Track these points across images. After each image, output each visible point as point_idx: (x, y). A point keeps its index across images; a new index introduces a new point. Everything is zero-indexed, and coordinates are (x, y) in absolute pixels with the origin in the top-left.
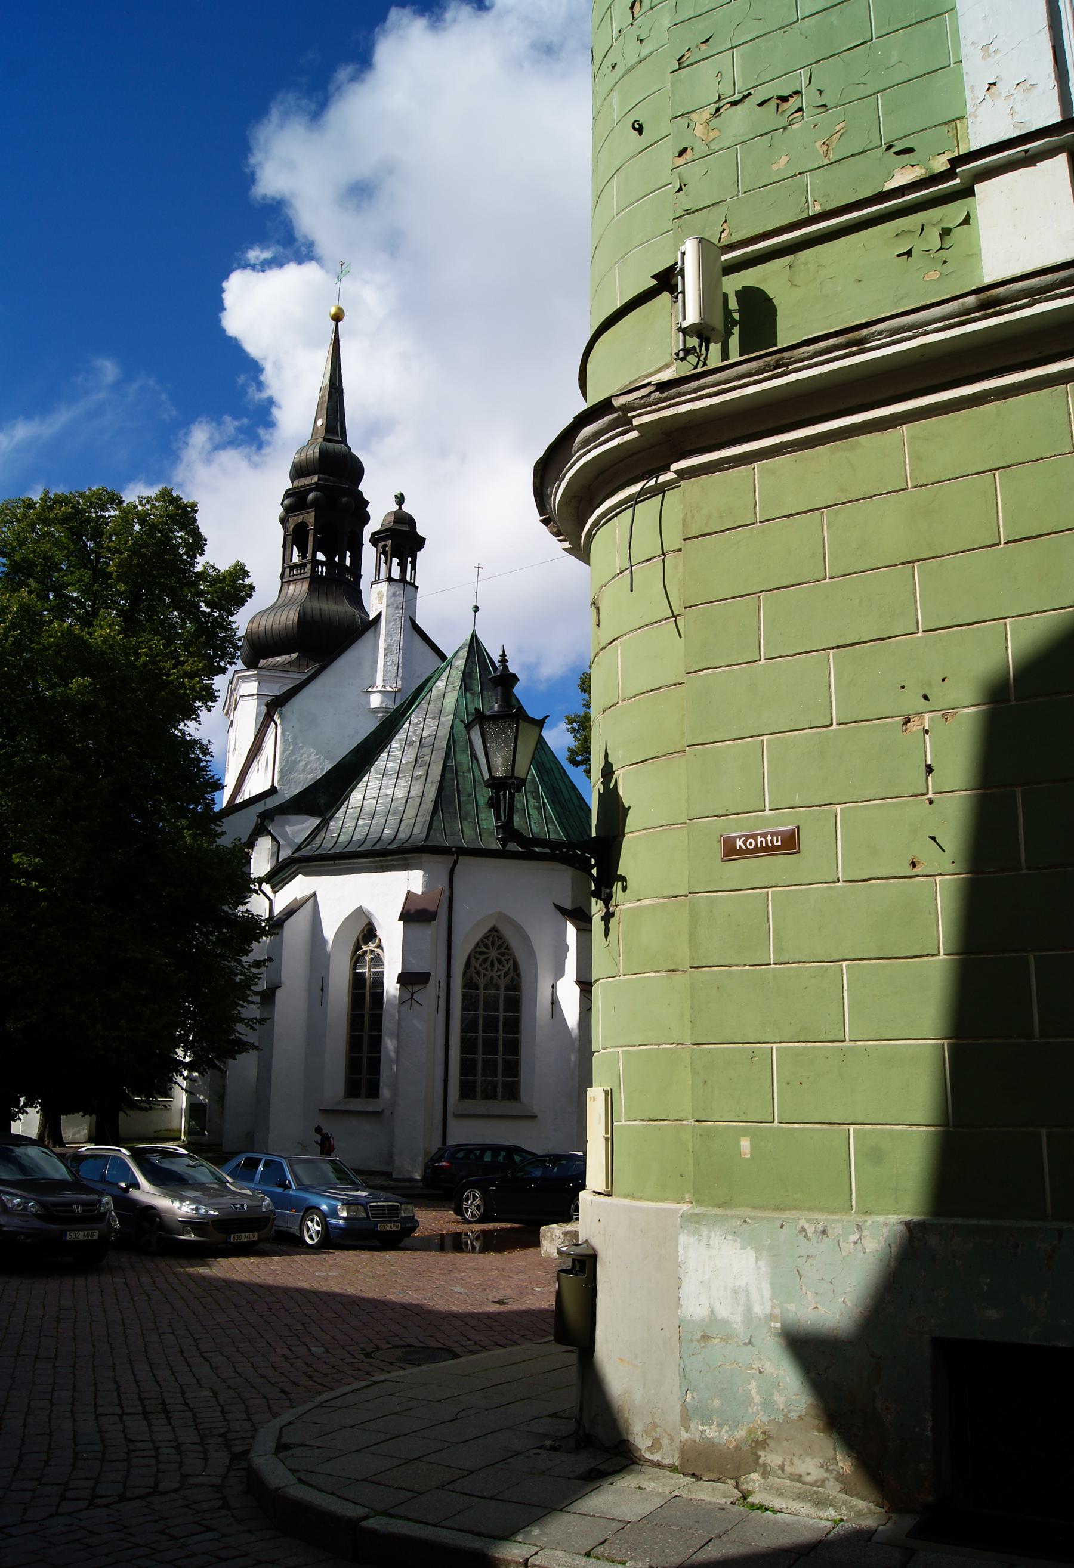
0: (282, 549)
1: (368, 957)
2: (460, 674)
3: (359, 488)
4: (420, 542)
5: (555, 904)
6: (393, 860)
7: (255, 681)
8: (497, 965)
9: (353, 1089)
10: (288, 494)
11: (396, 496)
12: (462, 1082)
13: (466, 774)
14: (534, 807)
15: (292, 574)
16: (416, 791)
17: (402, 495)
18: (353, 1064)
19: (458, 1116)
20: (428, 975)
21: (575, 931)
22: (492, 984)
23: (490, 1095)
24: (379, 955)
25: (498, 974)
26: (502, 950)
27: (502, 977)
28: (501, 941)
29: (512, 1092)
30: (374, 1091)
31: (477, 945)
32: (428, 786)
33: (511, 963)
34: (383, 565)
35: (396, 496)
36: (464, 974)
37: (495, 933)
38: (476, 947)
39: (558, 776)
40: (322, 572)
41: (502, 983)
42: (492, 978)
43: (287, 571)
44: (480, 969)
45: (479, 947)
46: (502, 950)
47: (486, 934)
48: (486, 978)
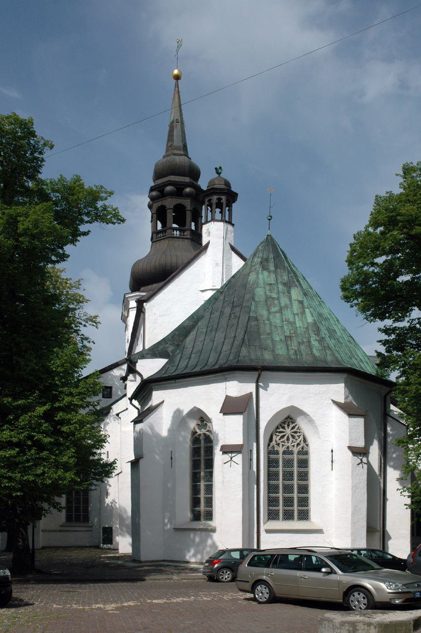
8: (291, 439)
14: (316, 340)
22: (288, 452)
25: (293, 444)
26: (295, 430)
33: (301, 437)
41: (296, 450)
42: (288, 447)
44: (279, 442)
46: (295, 430)
47: (283, 420)
48: (284, 447)
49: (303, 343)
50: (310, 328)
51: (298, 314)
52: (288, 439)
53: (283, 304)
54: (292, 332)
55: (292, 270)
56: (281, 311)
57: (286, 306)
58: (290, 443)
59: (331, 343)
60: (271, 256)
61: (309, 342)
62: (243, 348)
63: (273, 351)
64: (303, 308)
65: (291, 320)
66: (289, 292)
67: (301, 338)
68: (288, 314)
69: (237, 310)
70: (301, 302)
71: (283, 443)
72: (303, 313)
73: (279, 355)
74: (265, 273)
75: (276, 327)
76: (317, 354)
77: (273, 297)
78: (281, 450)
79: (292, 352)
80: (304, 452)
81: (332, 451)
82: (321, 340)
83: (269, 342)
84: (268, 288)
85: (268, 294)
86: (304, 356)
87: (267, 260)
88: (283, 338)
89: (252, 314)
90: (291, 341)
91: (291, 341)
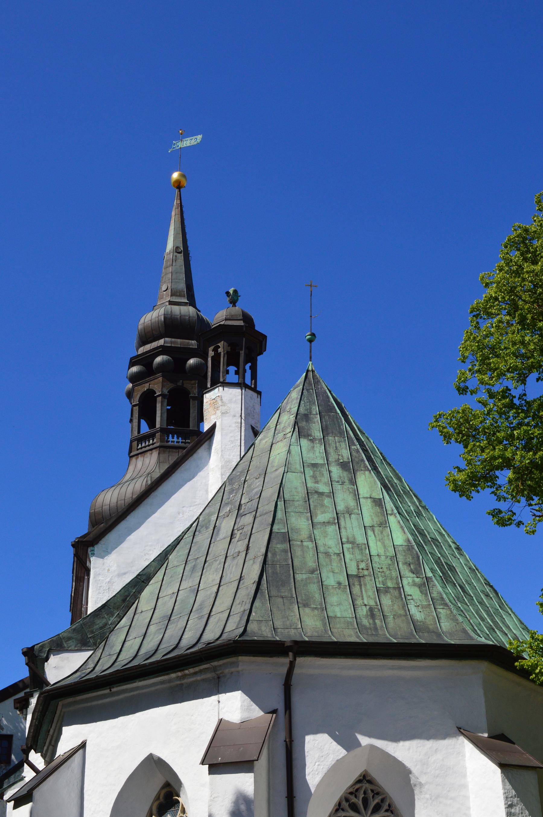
2: (292, 418)
6: (195, 673)
13: (305, 544)
14: (414, 584)
15: (140, 446)
16: (232, 573)
21: (498, 770)
37: (367, 785)
38: (337, 810)
43: (135, 443)
45: (343, 810)
47: (352, 786)
49: (387, 590)
50: (400, 558)
51: (372, 527)
53: (341, 507)
55: (359, 440)
56: (337, 520)
57: (349, 512)
60: (315, 409)
61: (399, 588)
62: (257, 603)
64: (385, 513)
65: (360, 539)
66: (353, 482)
67: (381, 579)
69: (248, 519)
70: (378, 503)
72: (384, 524)
73: (336, 617)
74: (304, 442)
75: (327, 554)
76: (418, 615)
77: (321, 490)
79: (363, 611)
84: (309, 472)
86: (390, 619)
87: (307, 417)
90: (361, 586)
91: (361, 586)
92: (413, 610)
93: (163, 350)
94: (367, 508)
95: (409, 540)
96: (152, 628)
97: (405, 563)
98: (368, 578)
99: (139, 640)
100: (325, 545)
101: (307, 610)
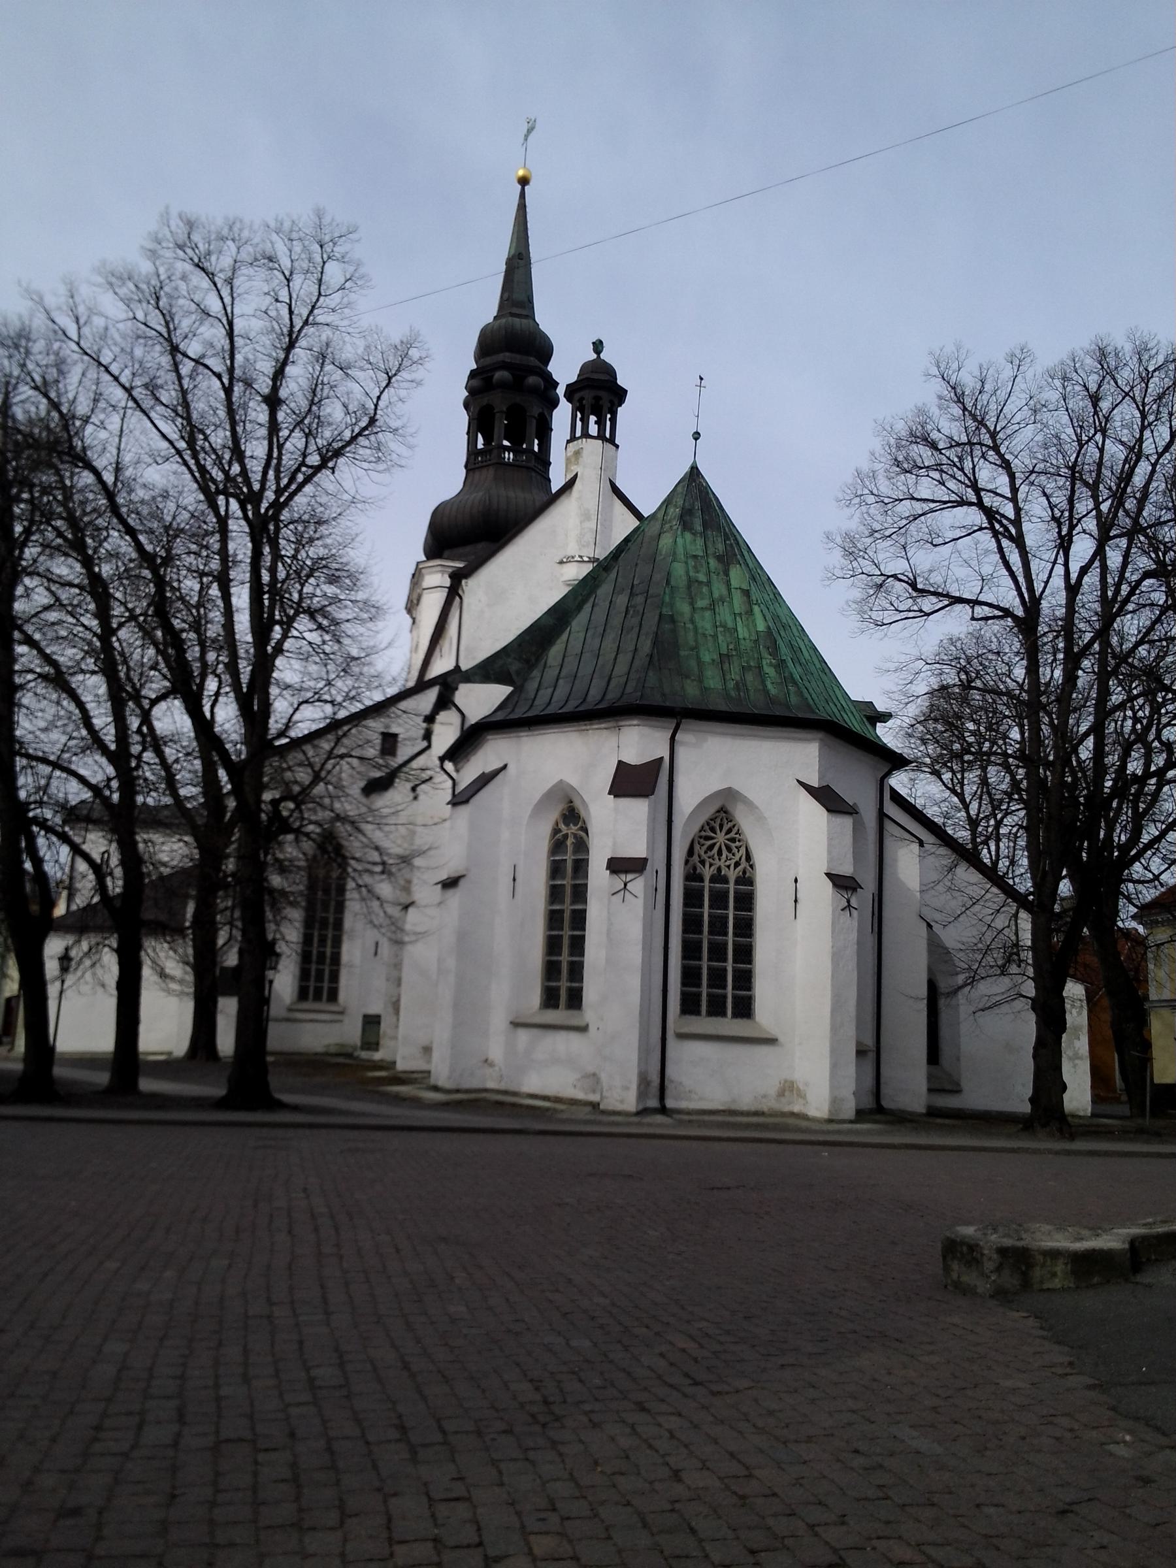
0: (466, 436)
1: (570, 841)
3: (549, 368)
4: (620, 395)
5: (798, 781)
7: (437, 572)
8: (725, 852)
9: (550, 999)
10: (473, 374)
11: (593, 343)
12: (683, 994)
14: (771, 665)
17: (601, 342)
18: (551, 970)
19: (682, 1036)
20: (645, 860)
22: (718, 878)
23: (717, 1009)
24: (581, 838)
25: (728, 863)
26: (732, 835)
27: (732, 867)
28: (730, 824)
29: (744, 1009)
30: (575, 1000)
31: (702, 829)
32: (642, 638)
33: (743, 850)
34: (579, 424)
35: (593, 343)
36: (687, 862)
38: (700, 831)
39: (796, 634)
40: (509, 459)
41: (732, 875)
42: (719, 869)
43: (473, 457)
44: (704, 856)
46: (732, 835)
50: (761, 642)
52: (720, 853)
53: (716, 595)
54: (731, 647)
56: (712, 607)
57: (722, 600)
58: (723, 860)
59: (796, 671)
60: (698, 505)
61: (760, 667)
62: (651, 673)
63: (700, 681)
65: (730, 624)
66: (727, 574)
68: (724, 614)
69: (639, 599)
70: (747, 593)
71: (711, 860)
72: (750, 612)
73: (710, 689)
74: (688, 536)
78: (708, 872)
79: (731, 685)
80: (746, 880)
81: (796, 881)
82: (780, 665)
83: (693, 663)
84: (691, 563)
85: (692, 574)
86: (752, 693)
88: (717, 657)
89: (665, 611)
92: (770, 686)
93: (504, 366)
94: (738, 598)
95: (769, 628)
96: (561, 682)
97: (764, 647)
98: (735, 658)
99: (550, 690)
100: (703, 627)
101: (689, 681)
